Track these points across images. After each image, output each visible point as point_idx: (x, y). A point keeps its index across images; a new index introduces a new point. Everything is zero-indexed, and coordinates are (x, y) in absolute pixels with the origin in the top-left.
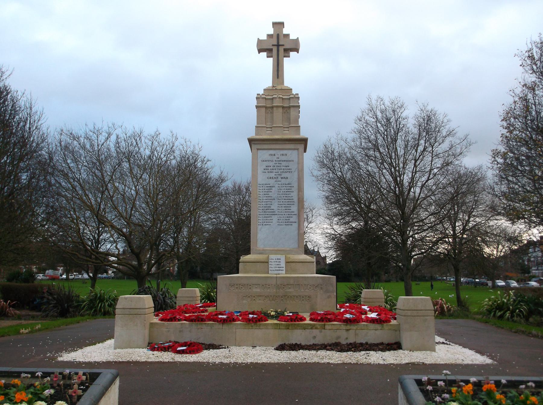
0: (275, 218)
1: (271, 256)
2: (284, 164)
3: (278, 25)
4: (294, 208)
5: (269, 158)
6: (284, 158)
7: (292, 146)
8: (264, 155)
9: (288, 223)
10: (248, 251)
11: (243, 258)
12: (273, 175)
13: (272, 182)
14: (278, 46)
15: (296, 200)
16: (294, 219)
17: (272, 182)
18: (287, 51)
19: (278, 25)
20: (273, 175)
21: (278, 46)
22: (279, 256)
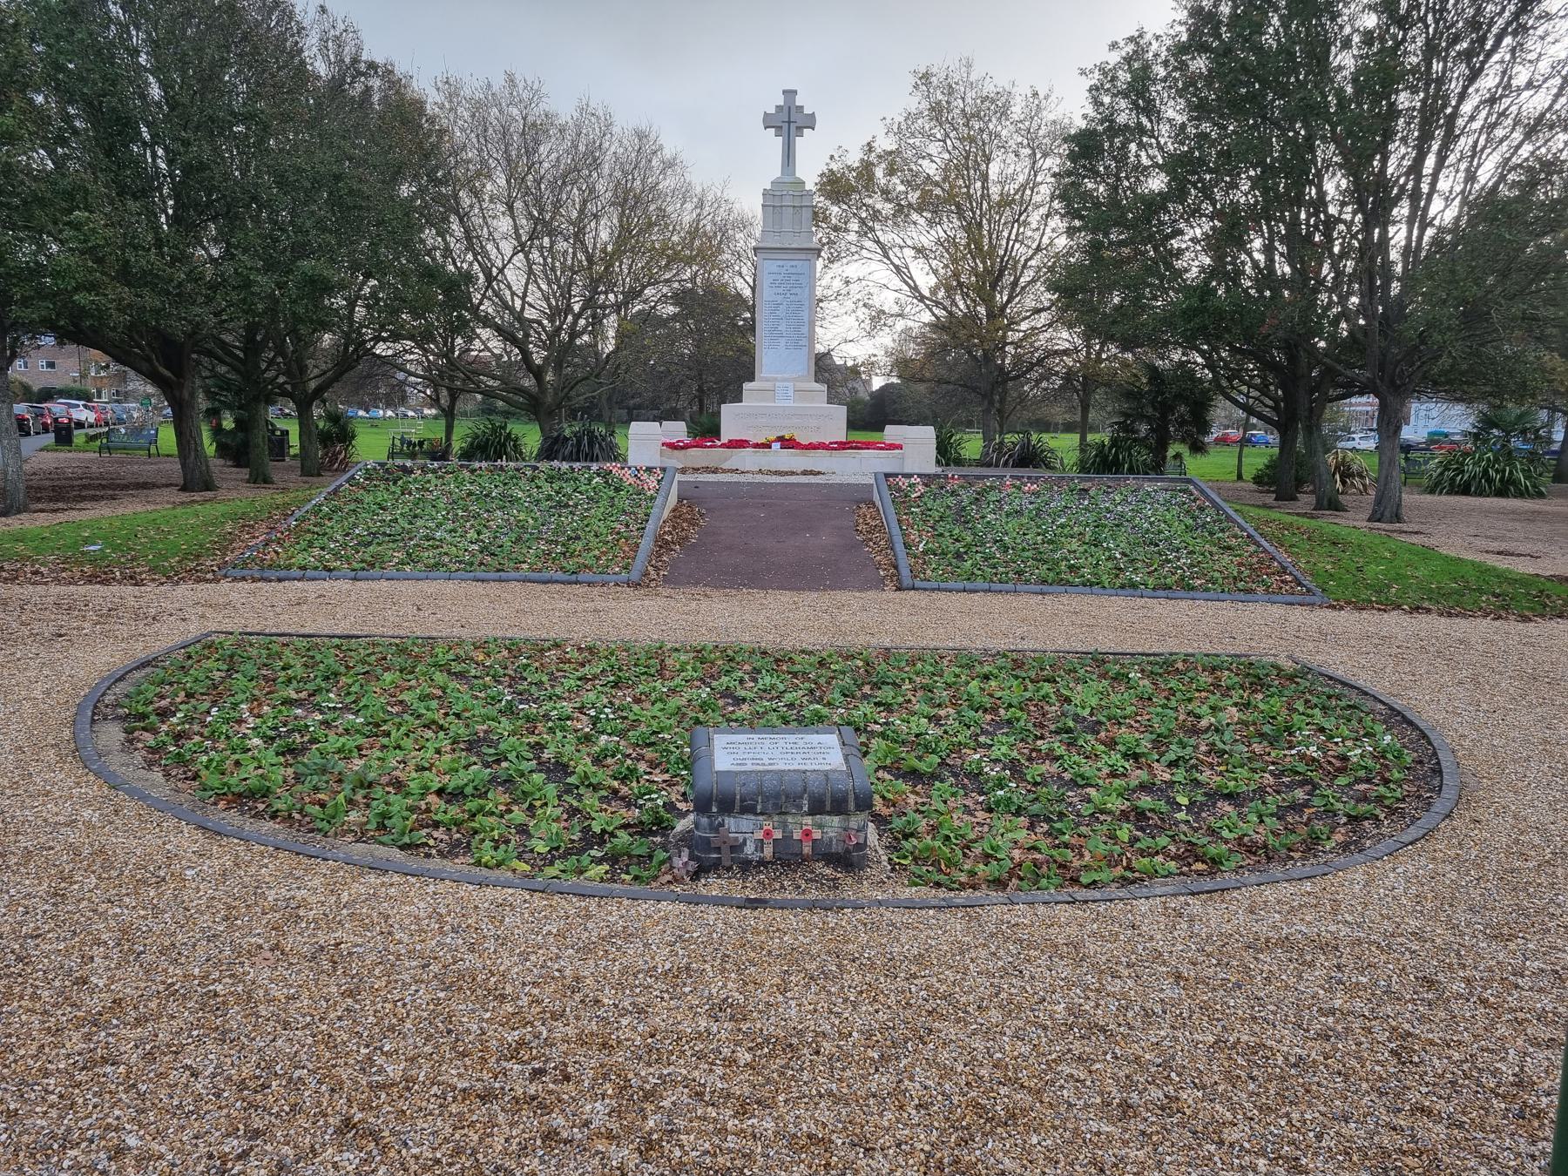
0: (783, 341)
1: (777, 384)
2: (794, 277)
3: (790, 94)
4: (805, 330)
5: (775, 269)
6: (793, 270)
7: (803, 256)
8: (770, 266)
9: (798, 347)
10: (751, 378)
11: (746, 386)
12: (780, 290)
13: (779, 298)
14: (789, 122)
15: (806, 320)
16: (804, 342)
17: (779, 298)
18: (800, 129)
19: (790, 94)
20: (780, 290)
21: (789, 122)
22: (786, 384)
